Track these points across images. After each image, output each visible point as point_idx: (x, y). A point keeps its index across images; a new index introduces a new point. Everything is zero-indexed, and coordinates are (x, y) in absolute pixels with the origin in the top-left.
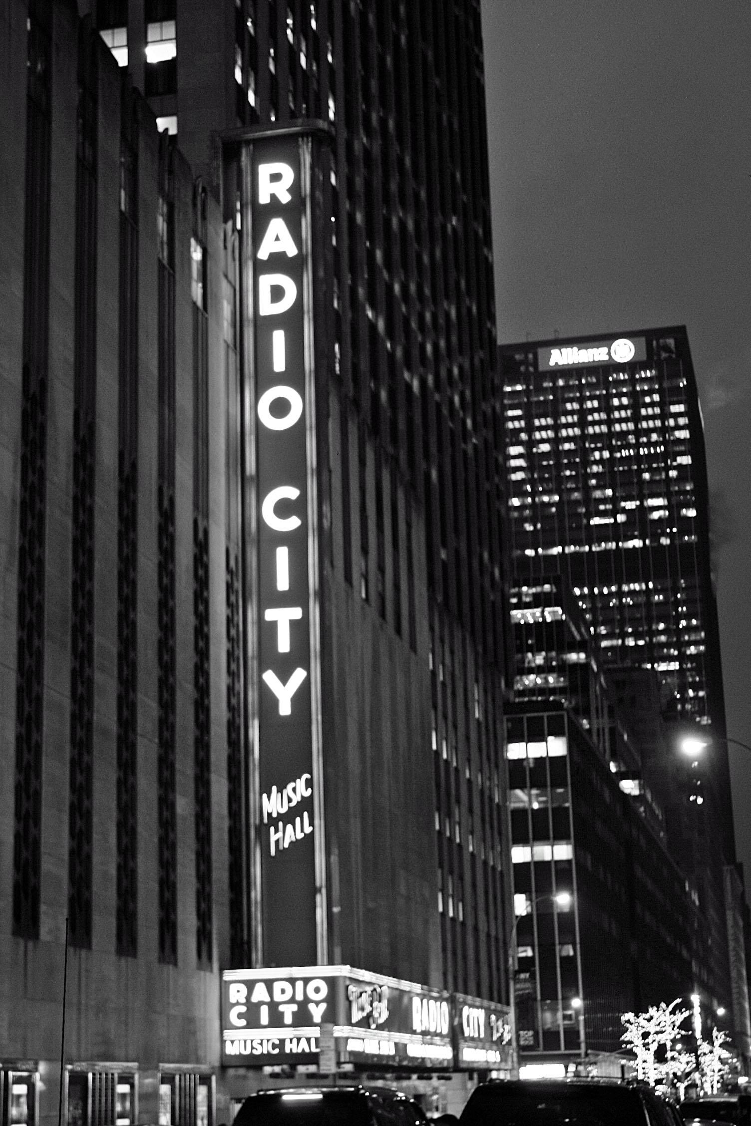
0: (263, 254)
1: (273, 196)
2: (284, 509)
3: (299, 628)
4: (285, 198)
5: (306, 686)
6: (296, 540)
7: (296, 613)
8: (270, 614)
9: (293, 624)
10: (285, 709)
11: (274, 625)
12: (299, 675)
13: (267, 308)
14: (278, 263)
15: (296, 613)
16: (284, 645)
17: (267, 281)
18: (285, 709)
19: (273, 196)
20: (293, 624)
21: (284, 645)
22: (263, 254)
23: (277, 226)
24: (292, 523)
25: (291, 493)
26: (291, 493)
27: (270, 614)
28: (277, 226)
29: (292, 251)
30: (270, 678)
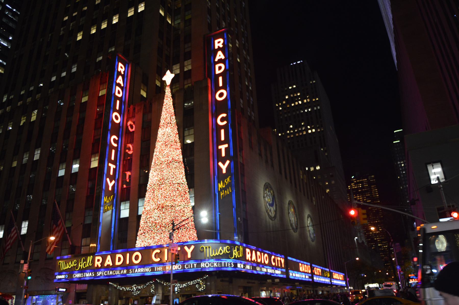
0: (118, 81)
1: (120, 71)
2: (114, 140)
3: (115, 170)
4: (123, 73)
5: (114, 184)
6: (116, 149)
7: (114, 167)
8: (110, 165)
9: (114, 168)
10: (110, 189)
11: (110, 167)
12: (113, 182)
13: (117, 94)
14: (119, 85)
15: (114, 167)
16: (111, 173)
17: (118, 88)
18: (110, 189)
19: (120, 71)
20: (114, 168)
21: (111, 173)
22: (118, 81)
23: (120, 78)
24: (115, 145)
25: (117, 139)
26: (117, 139)
27: (110, 165)
28: (120, 78)
29: (122, 85)
30: (108, 180)
